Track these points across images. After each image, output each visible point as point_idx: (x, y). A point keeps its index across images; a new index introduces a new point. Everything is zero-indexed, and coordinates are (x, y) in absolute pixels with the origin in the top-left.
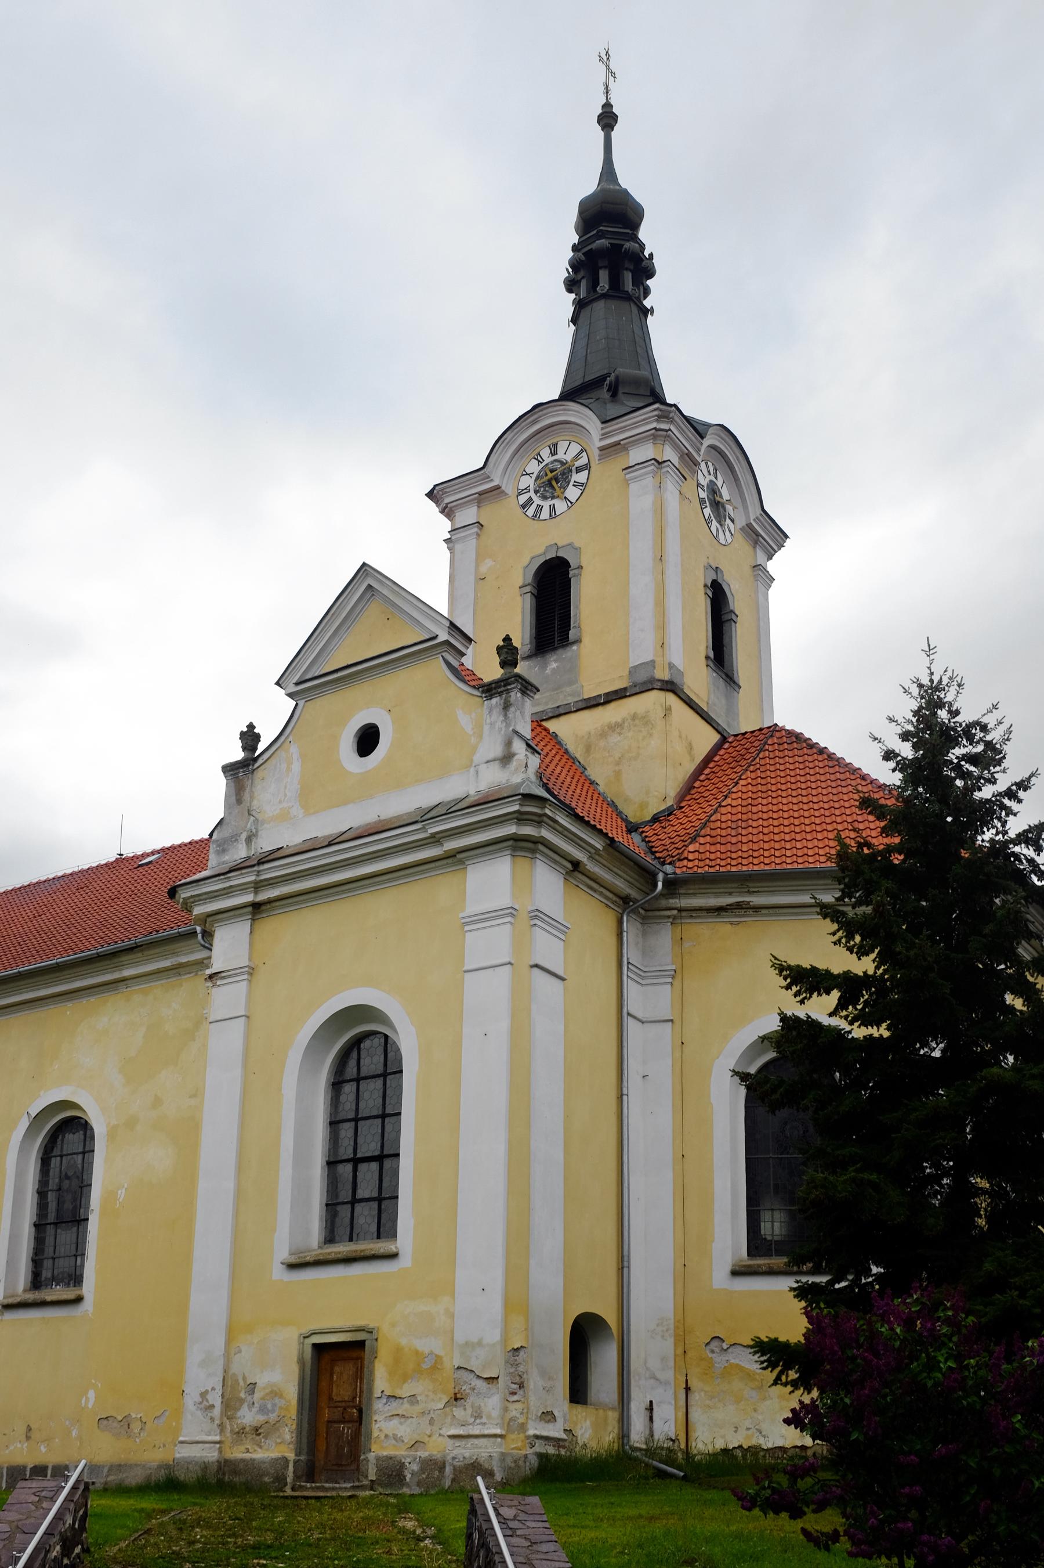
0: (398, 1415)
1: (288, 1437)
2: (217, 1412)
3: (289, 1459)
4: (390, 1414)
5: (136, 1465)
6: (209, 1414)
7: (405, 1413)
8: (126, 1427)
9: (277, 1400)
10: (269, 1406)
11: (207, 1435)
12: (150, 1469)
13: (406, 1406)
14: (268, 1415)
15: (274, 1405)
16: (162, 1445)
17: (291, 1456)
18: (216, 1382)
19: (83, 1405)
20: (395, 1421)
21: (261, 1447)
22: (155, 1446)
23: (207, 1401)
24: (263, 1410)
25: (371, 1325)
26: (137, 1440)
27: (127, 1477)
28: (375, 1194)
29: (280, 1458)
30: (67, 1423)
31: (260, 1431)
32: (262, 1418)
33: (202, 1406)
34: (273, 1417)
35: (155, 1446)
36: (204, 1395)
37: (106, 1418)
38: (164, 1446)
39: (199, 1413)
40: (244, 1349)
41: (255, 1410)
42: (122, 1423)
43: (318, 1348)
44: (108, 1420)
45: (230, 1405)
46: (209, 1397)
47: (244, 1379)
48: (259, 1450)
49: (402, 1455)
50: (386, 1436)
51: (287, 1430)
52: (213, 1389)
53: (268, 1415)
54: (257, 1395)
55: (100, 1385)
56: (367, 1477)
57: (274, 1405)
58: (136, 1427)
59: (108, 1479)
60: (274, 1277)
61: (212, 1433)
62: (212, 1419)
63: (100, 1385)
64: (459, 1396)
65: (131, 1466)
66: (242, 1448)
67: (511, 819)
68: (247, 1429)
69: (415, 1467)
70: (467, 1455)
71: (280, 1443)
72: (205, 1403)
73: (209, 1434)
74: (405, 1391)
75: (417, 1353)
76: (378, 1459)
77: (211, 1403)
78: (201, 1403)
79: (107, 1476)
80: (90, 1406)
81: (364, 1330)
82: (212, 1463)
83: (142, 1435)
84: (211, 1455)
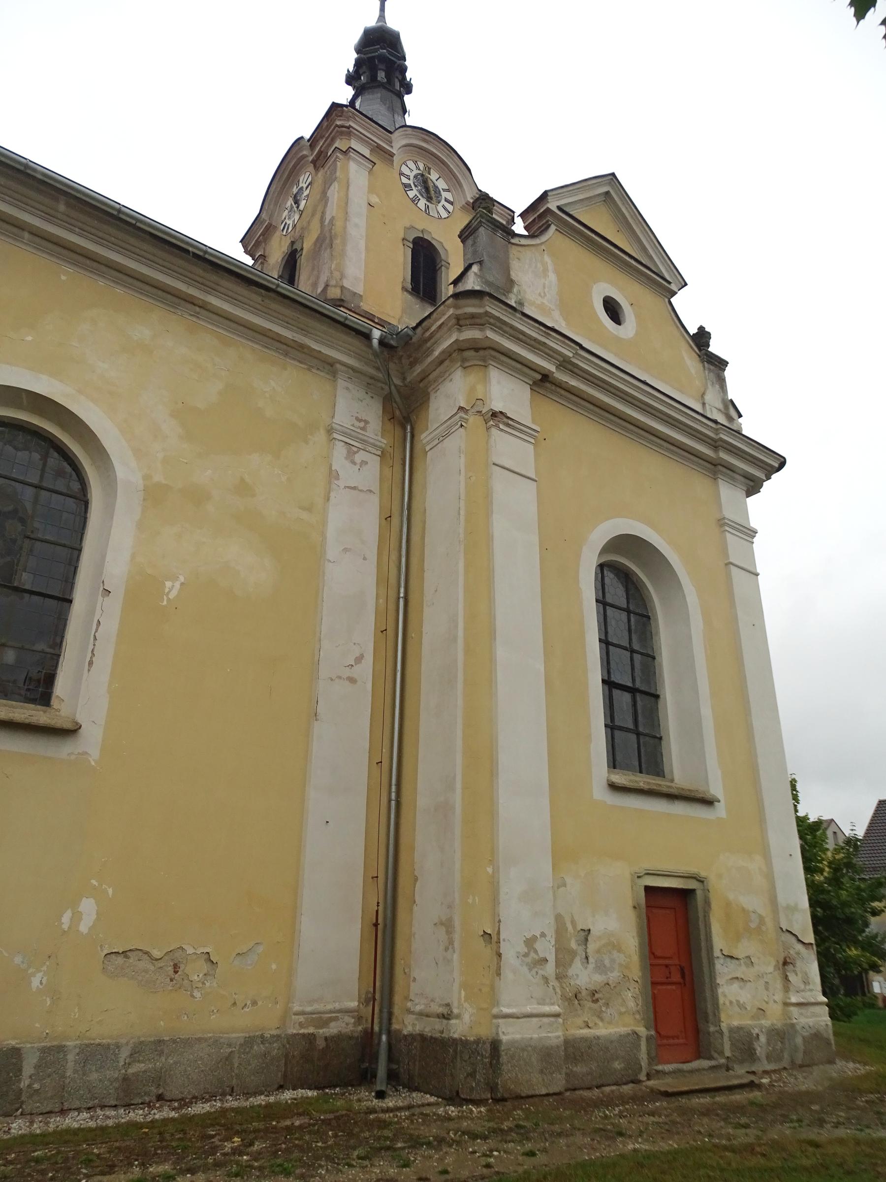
0: (737, 978)
1: (631, 1004)
2: (550, 969)
3: (640, 1034)
4: (730, 977)
5: (199, 1040)
6: (540, 972)
7: (743, 977)
8: (170, 969)
9: (615, 954)
10: (607, 962)
11: (539, 1004)
12: (230, 1045)
13: (744, 968)
14: (606, 974)
15: (613, 961)
16: (249, 1003)
17: (642, 1031)
18: (547, 925)
19: (65, 927)
20: (736, 986)
21: (602, 1020)
22: (235, 1004)
23: (536, 952)
24: (601, 968)
25: (703, 874)
26: (197, 994)
27: (175, 1063)
28: (617, 723)
29: (629, 1034)
30: (18, 960)
31: (597, 996)
32: (599, 978)
33: (529, 960)
34: (614, 976)
35: (235, 1004)
36: (530, 942)
37: (123, 953)
38: (254, 1003)
39: (525, 969)
40: (569, 880)
41: (591, 966)
42: (160, 964)
43: (648, 889)
44: (127, 957)
45: (564, 958)
46: (538, 946)
47: (573, 922)
48: (601, 1024)
49: (750, 1025)
50: (731, 1002)
51: (630, 995)
52: (543, 935)
53: (606, 974)
54: (592, 947)
55: (110, 891)
56: (721, 1053)
57: (613, 961)
58: (195, 971)
59: (130, 1071)
60: (595, 797)
61: (548, 1001)
62: (546, 980)
63: (110, 891)
64: (788, 960)
65: (187, 1043)
66: (579, 1021)
67: (765, 469)
68: (584, 993)
69: (763, 1039)
70: (811, 1024)
71: (625, 1012)
72: (533, 955)
73: (542, 1002)
74: (740, 951)
75: (743, 909)
76: (731, 1030)
77: (542, 955)
78: (526, 955)
79: (127, 1065)
80: (84, 928)
81: (695, 878)
82: (558, 1047)
83: (208, 984)
84: (554, 1035)
